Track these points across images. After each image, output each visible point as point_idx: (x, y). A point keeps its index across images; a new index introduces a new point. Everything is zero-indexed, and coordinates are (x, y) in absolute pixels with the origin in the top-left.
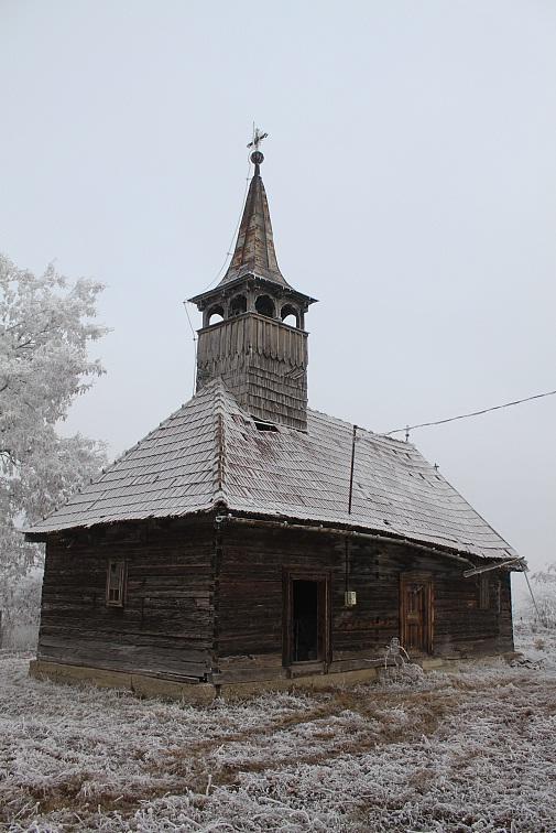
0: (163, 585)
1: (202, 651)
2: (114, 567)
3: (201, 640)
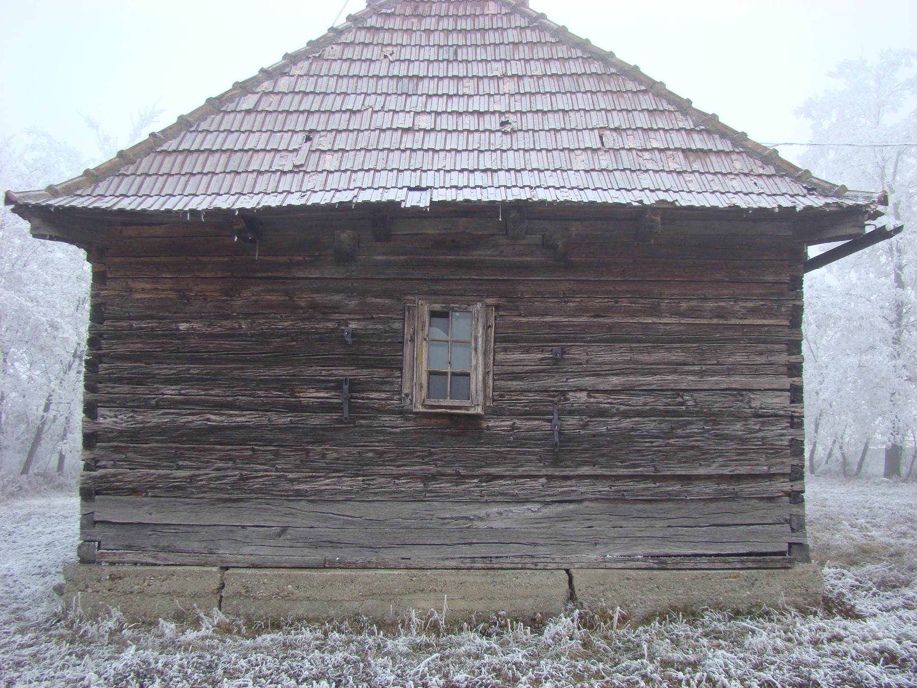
0: (636, 362)
1: (771, 499)
3: (769, 477)
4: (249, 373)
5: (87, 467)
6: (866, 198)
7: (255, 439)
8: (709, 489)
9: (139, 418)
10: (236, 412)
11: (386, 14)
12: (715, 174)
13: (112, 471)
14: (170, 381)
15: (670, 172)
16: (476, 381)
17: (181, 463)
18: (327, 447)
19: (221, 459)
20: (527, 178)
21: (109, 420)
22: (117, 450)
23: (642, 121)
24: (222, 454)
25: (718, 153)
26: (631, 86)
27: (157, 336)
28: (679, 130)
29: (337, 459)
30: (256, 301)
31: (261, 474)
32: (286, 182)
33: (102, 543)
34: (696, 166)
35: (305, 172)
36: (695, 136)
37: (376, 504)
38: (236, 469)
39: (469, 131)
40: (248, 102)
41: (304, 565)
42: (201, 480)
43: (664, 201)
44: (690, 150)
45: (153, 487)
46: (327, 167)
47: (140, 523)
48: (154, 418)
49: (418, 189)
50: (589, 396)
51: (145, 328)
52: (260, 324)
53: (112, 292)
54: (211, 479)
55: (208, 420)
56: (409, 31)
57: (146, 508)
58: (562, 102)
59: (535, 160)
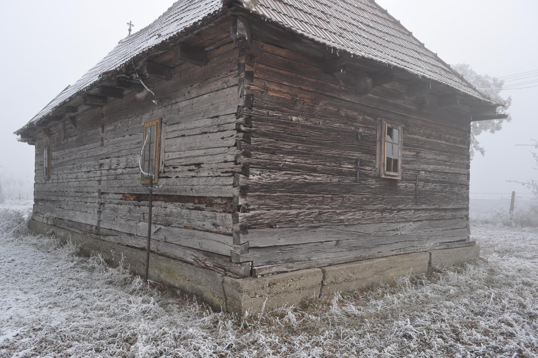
2: (390, 132)
4: (323, 152)
7: (324, 191)
8: (449, 214)
9: (273, 176)
10: (317, 175)
13: (258, 212)
14: (289, 153)
17: (292, 205)
18: (350, 195)
19: (310, 203)
21: (256, 177)
22: (259, 197)
24: (310, 199)
27: (281, 123)
29: (354, 202)
30: (325, 109)
31: (326, 211)
33: (254, 262)
37: (367, 225)
38: (316, 208)
41: (348, 261)
42: (301, 216)
45: (279, 222)
47: (274, 246)
48: (280, 177)
50: (425, 173)
51: (275, 116)
52: (328, 123)
53: (257, 88)
54: (306, 215)
55: (305, 179)
57: (276, 235)
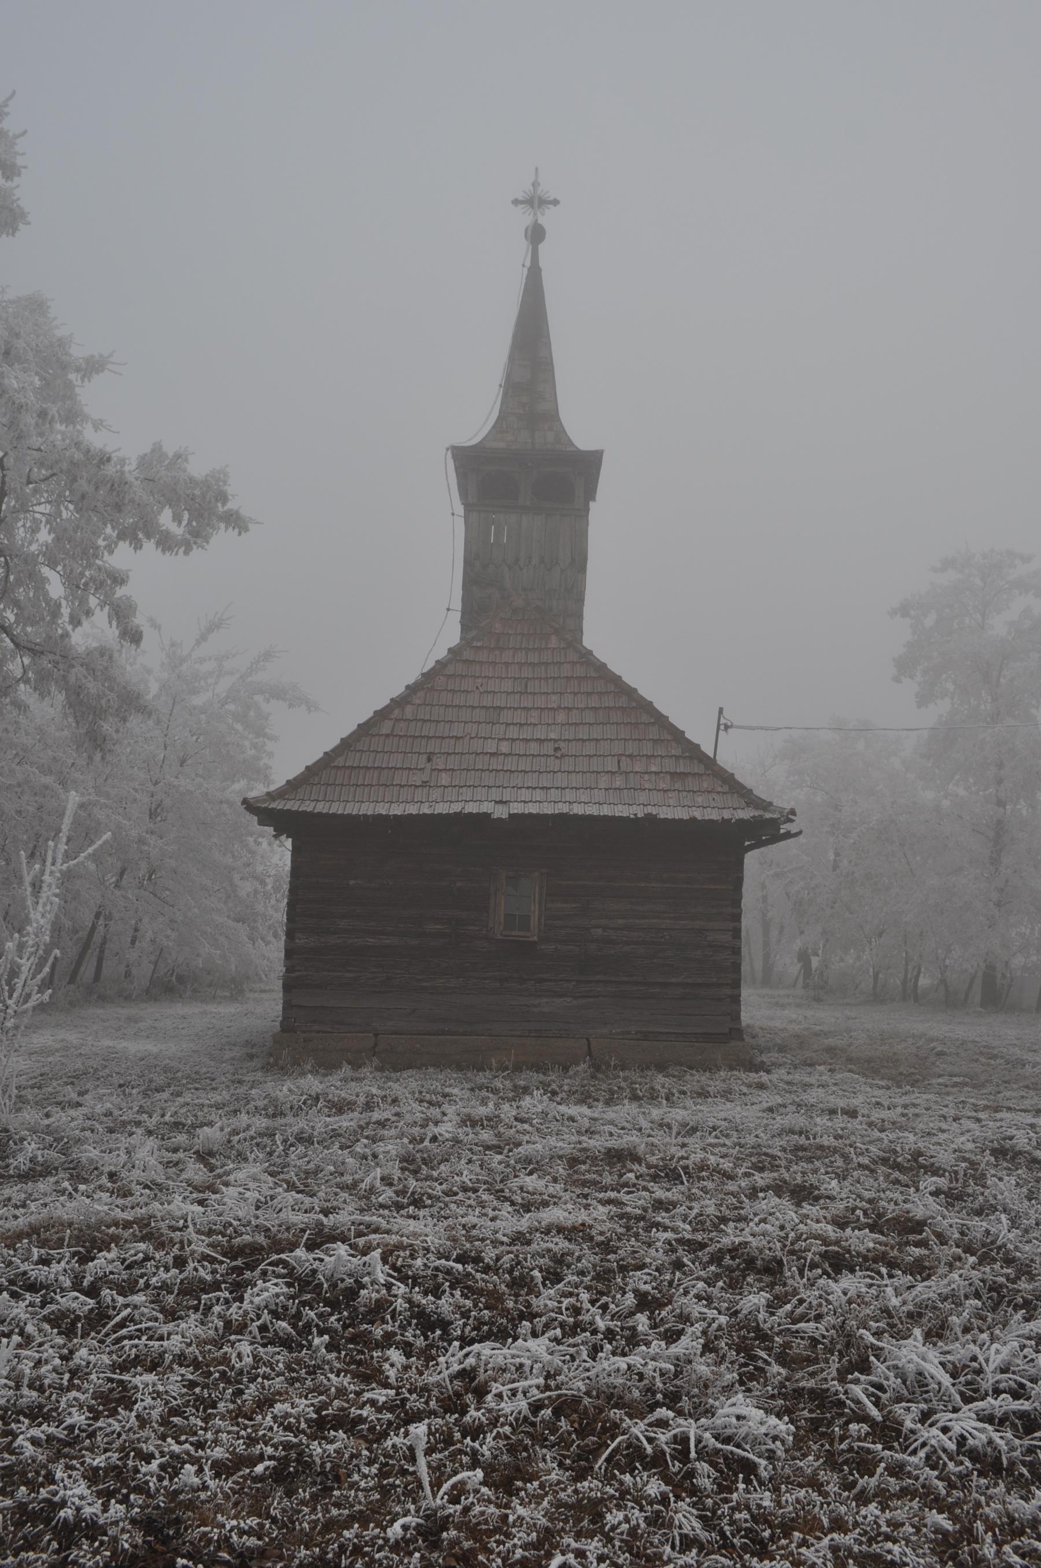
5: (287, 971)
6: (780, 812)
9: (323, 940)
11: (477, 647)
12: (689, 791)
15: (659, 790)
16: (534, 921)
20: (569, 795)
23: (647, 749)
25: (694, 775)
26: (645, 718)
28: (671, 756)
32: (420, 794)
34: (677, 786)
35: (430, 787)
36: (681, 761)
39: (533, 755)
40: (386, 728)
43: (650, 814)
44: (676, 773)
46: (444, 783)
49: (501, 802)
56: (494, 663)
58: (596, 732)
59: (575, 780)
